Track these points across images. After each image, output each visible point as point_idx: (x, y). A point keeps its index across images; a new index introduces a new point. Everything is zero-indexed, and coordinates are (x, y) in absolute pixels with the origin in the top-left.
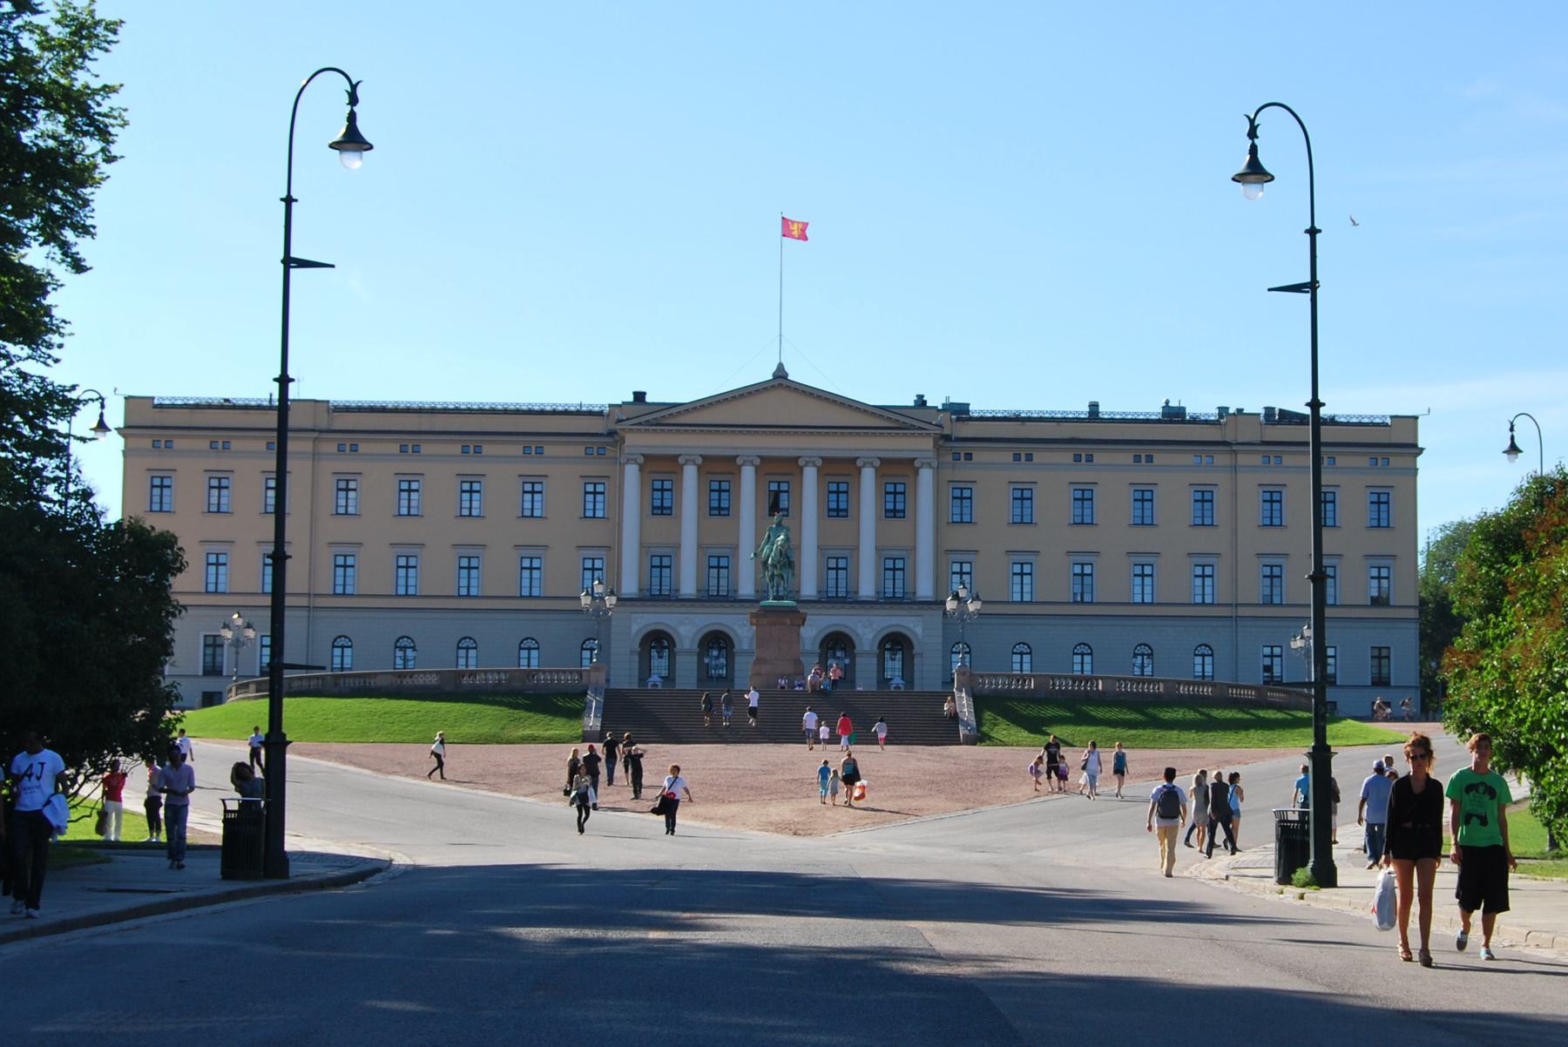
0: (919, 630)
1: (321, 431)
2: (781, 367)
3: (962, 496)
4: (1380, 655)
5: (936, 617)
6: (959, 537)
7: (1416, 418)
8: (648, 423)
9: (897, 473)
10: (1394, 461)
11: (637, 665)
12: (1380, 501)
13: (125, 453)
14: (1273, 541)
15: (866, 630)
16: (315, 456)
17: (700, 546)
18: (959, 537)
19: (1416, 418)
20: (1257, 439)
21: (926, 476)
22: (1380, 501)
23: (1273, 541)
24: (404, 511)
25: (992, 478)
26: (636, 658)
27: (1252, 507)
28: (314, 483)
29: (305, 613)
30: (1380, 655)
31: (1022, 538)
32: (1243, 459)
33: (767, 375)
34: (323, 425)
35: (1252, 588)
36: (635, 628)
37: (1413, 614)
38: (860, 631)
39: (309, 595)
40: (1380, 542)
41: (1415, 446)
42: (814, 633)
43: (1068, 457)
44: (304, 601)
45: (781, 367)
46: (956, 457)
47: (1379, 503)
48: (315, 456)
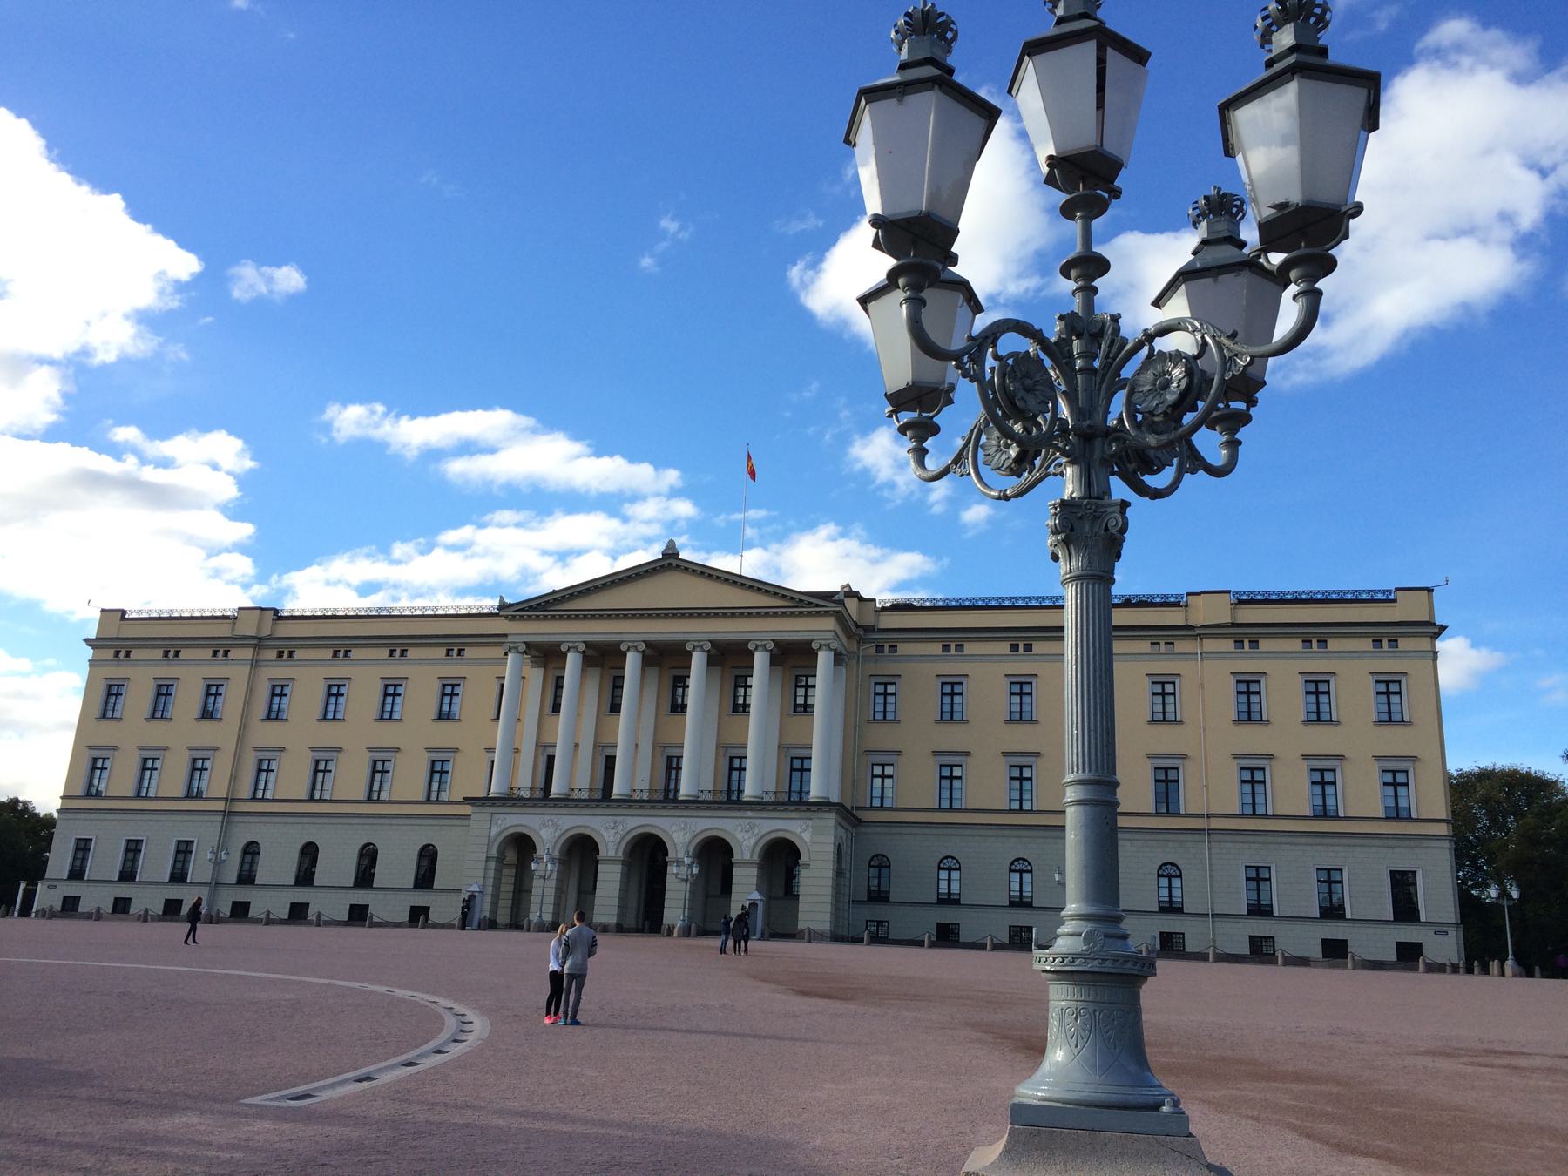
0: (807, 836)
1: (260, 639)
2: (671, 544)
3: (884, 688)
4: (1403, 884)
5: (830, 820)
6: (882, 737)
7: (1430, 590)
8: (531, 608)
9: (793, 659)
10: (1404, 644)
11: (491, 873)
12: (1388, 688)
13: (92, 663)
14: (1253, 739)
15: (746, 837)
16: (255, 663)
17: (596, 746)
18: (882, 737)
19: (1430, 590)
20: (1227, 620)
21: (824, 659)
22: (1388, 688)
23: (1253, 739)
24: (330, 715)
25: (921, 672)
26: (492, 865)
27: (1227, 702)
28: (250, 691)
29: (220, 818)
30: (1403, 884)
31: (951, 738)
32: (1210, 645)
33: (653, 553)
34: (266, 632)
35: (1227, 795)
36: (494, 831)
37: (1443, 829)
38: (740, 836)
39: (226, 799)
40: (1394, 741)
41: (1431, 624)
42: (688, 837)
43: (1004, 648)
44: (220, 806)
45: (671, 544)
46: (879, 648)
47: (1388, 693)
48: (255, 663)
